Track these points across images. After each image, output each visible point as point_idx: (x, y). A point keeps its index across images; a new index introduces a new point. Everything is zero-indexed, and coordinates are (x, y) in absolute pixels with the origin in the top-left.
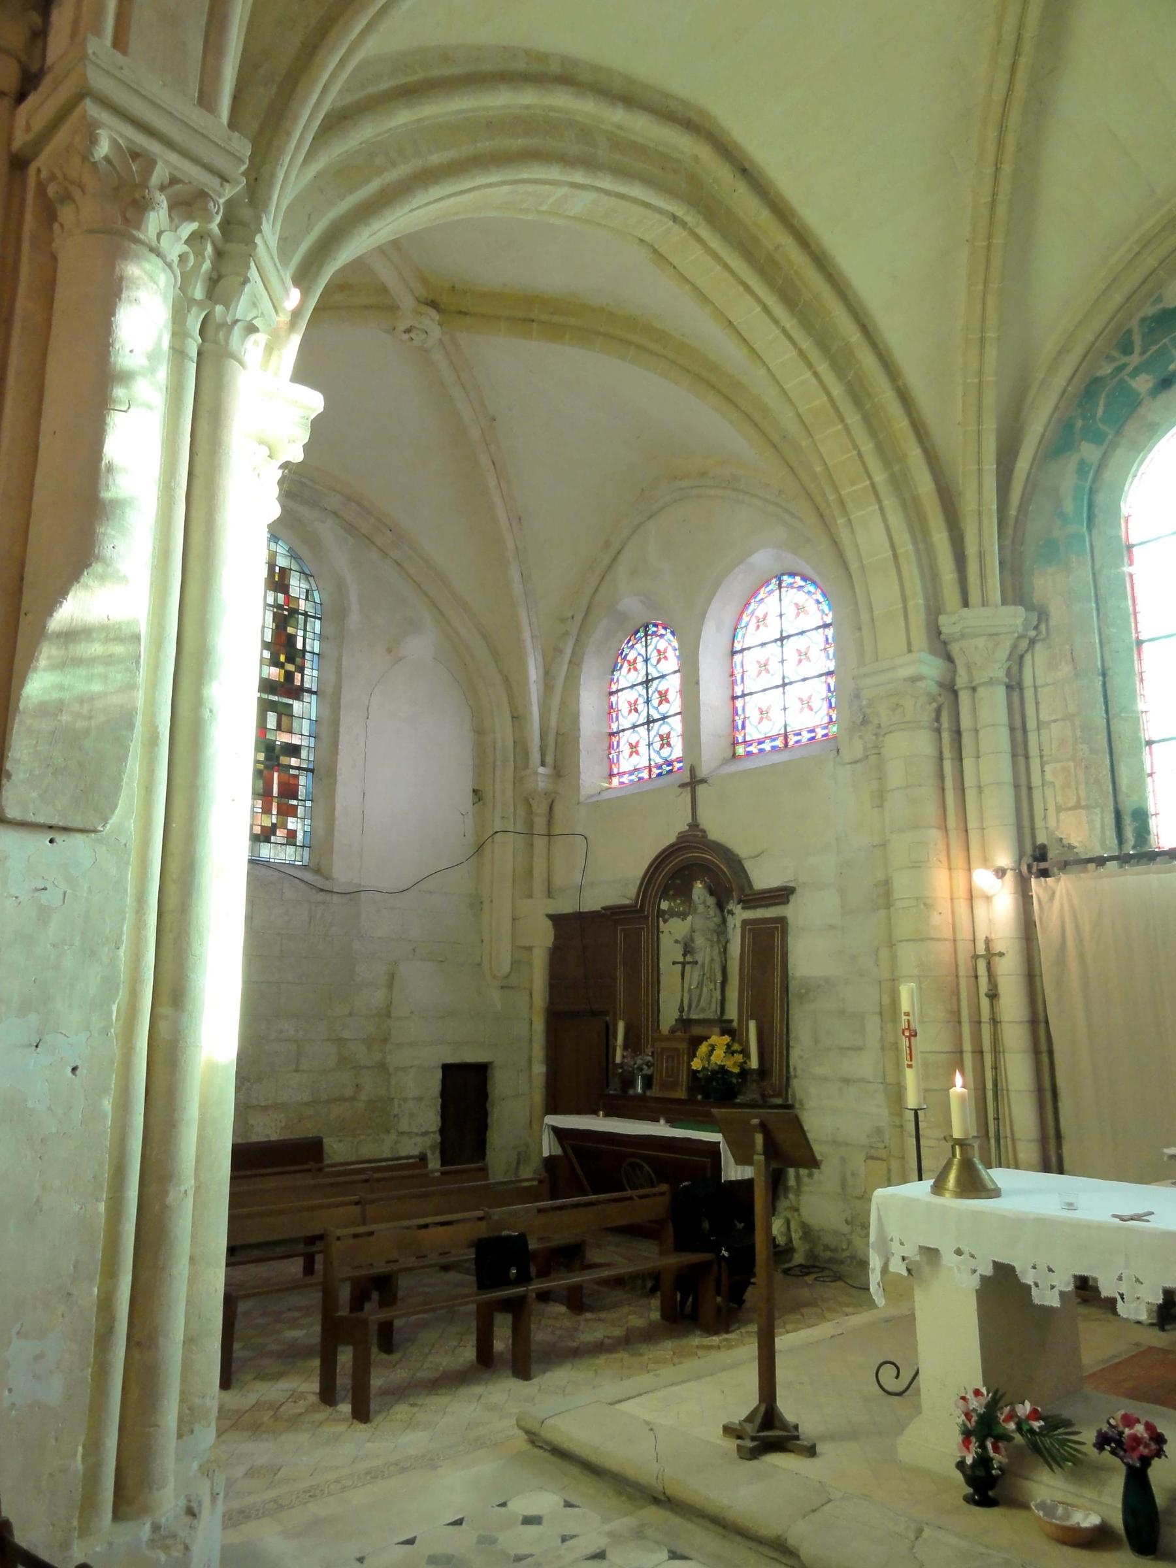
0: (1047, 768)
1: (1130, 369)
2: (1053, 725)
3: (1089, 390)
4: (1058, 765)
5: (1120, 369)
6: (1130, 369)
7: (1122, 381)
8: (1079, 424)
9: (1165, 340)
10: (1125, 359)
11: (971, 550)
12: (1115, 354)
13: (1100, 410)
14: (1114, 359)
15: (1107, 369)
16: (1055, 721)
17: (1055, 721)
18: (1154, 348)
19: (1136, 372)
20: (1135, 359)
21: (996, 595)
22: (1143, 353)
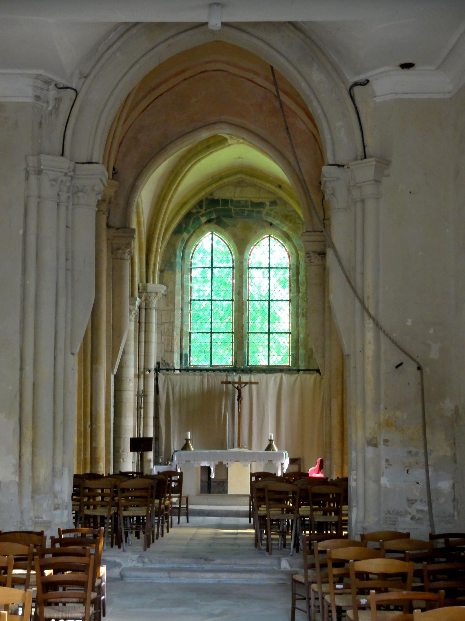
0: (162, 337)
1: (201, 214)
2: (166, 324)
3: (189, 215)
4: (166, 337)
5: (198, 212)
6: (201, 214)
7: (198, 216)
8: (184, 226)
9: (212, 209)
10: (200, 210)
11: (152, 263)
12: (198, 207)
13: (191, 223)
14: (197, 209)
15: (195, 211)
16: (167, 323)
17: (167, 323)
18: (209, 210)
19: (202, 216)
20: (203, 211)
21: (157, 279)
22: (205, 210)
